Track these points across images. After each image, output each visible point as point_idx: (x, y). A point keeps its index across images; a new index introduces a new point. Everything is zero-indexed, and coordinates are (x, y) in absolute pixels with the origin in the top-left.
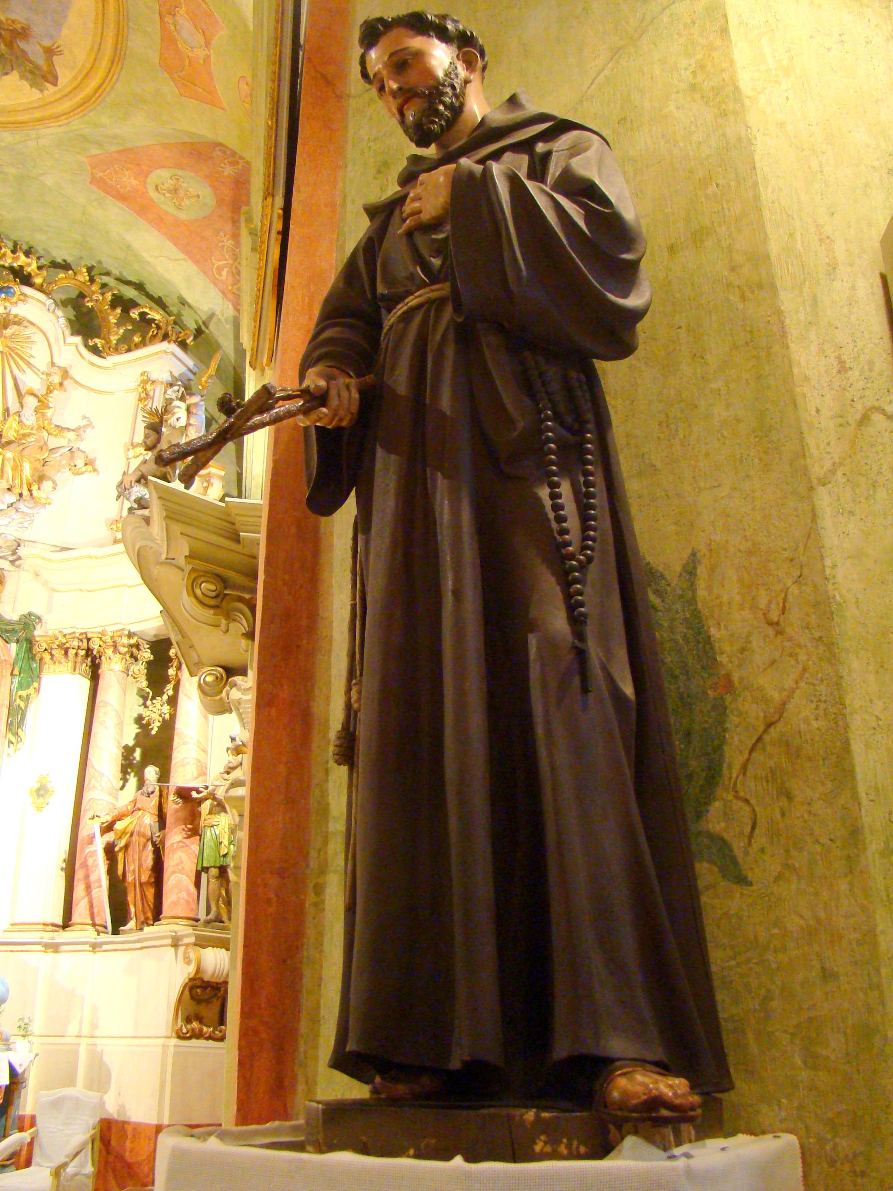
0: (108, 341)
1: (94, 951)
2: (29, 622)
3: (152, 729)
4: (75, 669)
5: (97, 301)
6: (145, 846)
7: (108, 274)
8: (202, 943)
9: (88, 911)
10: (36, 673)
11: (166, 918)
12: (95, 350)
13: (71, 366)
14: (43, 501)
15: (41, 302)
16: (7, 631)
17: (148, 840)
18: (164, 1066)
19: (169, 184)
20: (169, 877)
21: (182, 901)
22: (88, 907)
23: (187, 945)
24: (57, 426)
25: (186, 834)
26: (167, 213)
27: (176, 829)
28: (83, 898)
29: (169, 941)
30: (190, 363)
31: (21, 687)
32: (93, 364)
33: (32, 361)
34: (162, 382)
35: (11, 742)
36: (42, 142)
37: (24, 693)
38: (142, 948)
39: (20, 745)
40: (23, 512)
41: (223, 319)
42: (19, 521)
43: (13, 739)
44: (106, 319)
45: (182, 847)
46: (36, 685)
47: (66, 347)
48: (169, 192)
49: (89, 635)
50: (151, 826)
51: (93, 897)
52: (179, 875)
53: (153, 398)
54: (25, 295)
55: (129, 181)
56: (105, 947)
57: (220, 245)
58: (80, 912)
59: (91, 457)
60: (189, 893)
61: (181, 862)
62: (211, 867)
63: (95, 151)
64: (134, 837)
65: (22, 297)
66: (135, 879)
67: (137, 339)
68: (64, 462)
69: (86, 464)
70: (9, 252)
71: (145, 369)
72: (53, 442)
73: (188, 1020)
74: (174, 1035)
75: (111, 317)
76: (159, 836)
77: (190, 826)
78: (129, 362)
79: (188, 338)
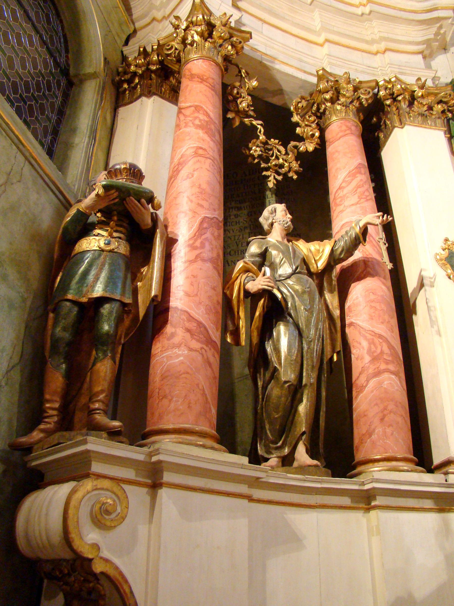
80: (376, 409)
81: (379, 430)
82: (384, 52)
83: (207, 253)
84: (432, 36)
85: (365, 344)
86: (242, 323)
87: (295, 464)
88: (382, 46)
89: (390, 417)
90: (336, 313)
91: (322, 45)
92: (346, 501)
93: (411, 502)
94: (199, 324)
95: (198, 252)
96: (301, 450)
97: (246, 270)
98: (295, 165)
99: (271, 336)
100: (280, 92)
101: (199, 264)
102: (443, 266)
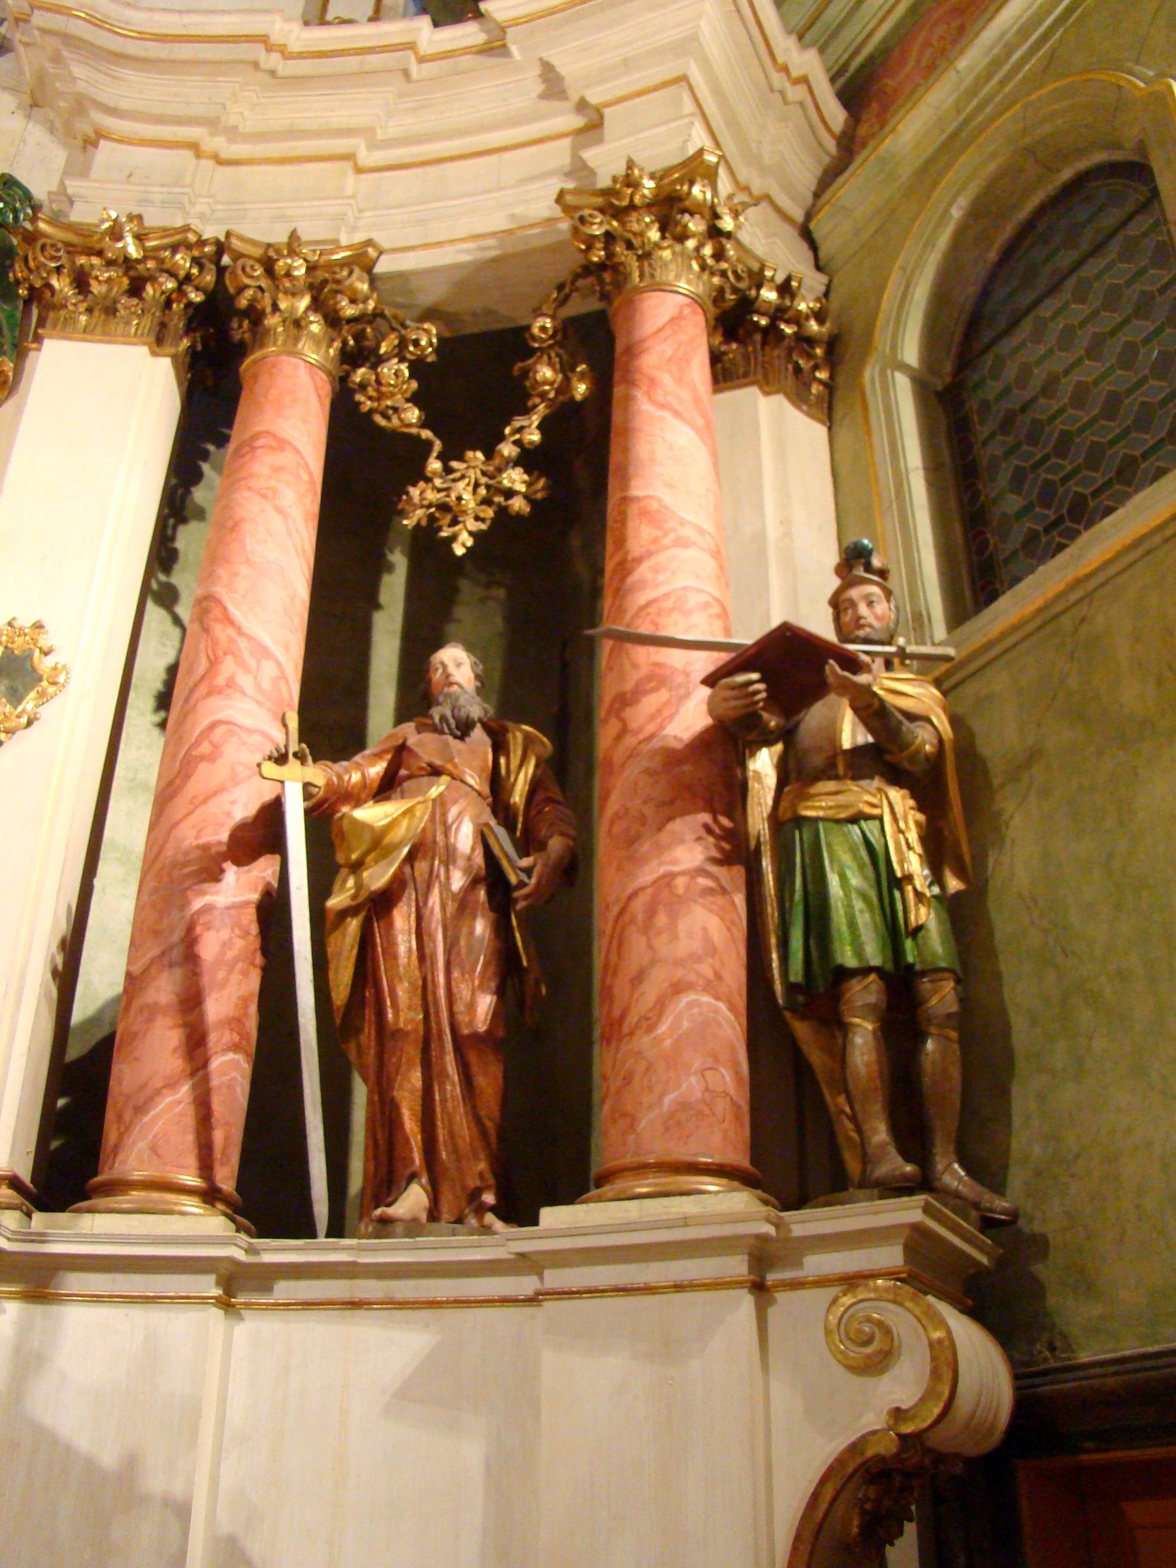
1: (226, 1304)
3: (453, 538)
9: (190, 1137)
11: (642, 1169)
20: (661, 1005)
21: (722, 1106)
22: (190, 1120)
25: (721, 849)
27: (677, 825)
28: (171, 1085)
29: (737, 1266)
45: (708, 891)
51: (215, 1082)
52: (706, 999)
56: (284, 1290)
62: (865, 971)
64: (421, 866)
76: (528, 871)
77: (725, 821)
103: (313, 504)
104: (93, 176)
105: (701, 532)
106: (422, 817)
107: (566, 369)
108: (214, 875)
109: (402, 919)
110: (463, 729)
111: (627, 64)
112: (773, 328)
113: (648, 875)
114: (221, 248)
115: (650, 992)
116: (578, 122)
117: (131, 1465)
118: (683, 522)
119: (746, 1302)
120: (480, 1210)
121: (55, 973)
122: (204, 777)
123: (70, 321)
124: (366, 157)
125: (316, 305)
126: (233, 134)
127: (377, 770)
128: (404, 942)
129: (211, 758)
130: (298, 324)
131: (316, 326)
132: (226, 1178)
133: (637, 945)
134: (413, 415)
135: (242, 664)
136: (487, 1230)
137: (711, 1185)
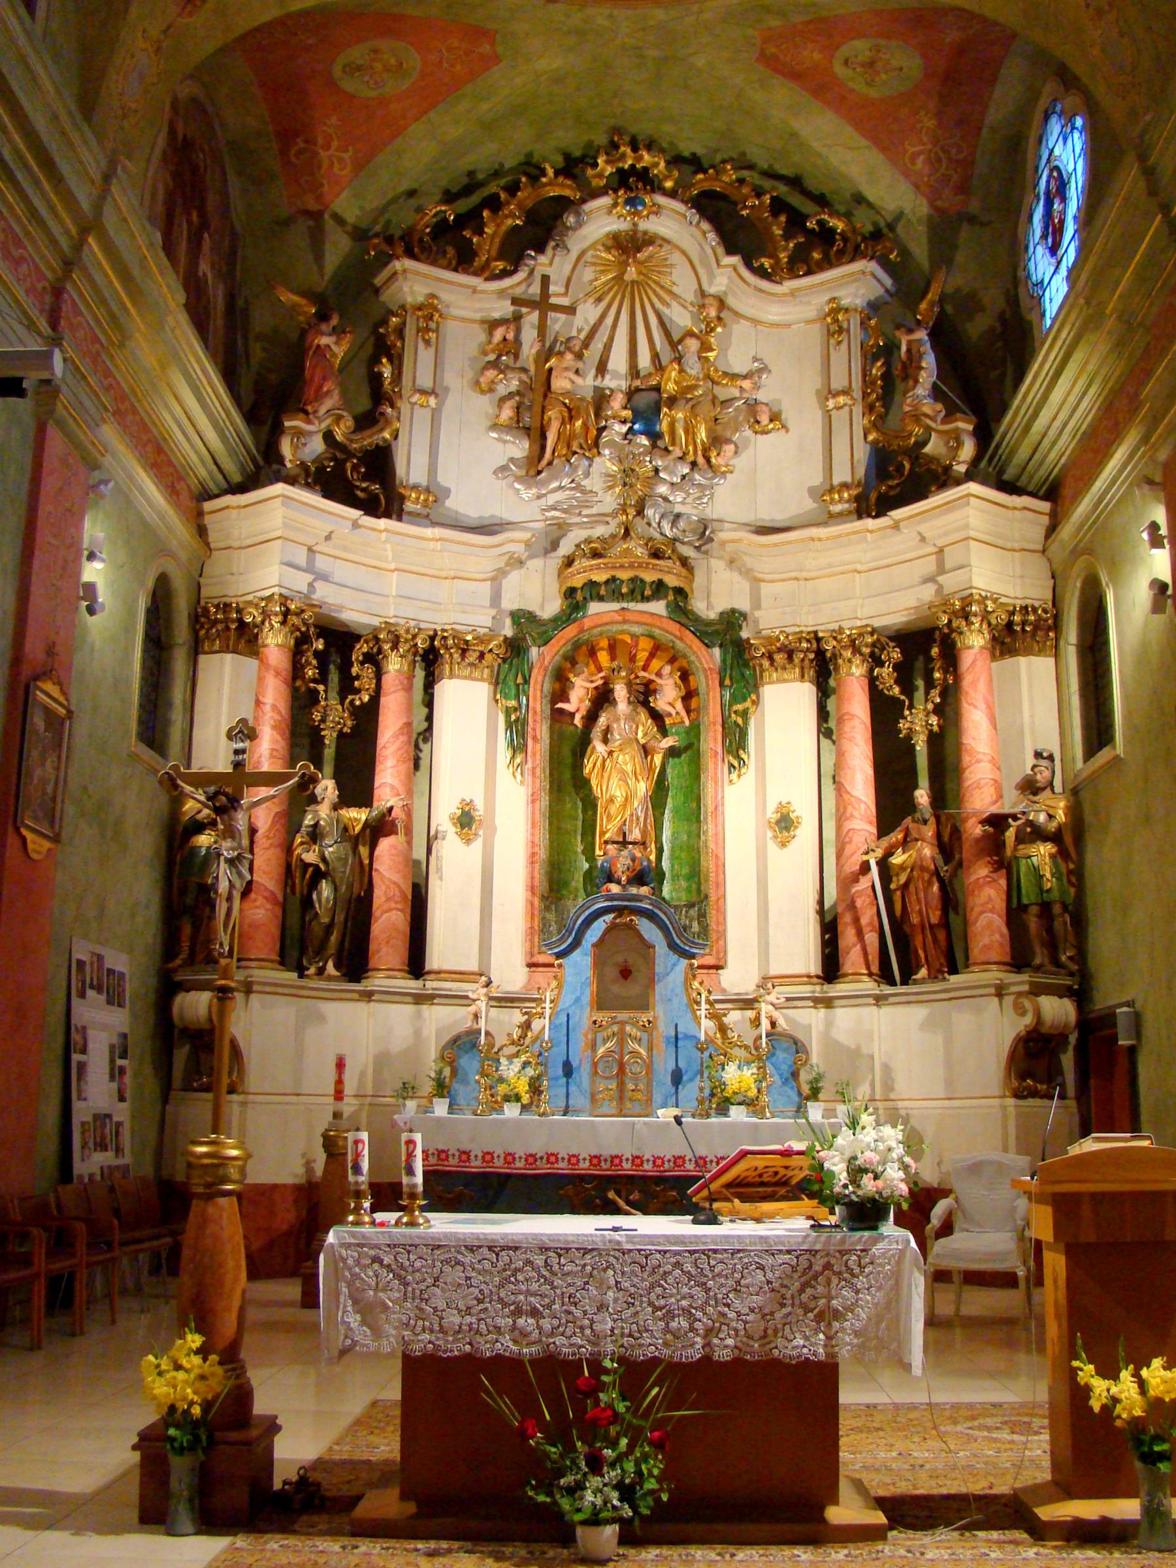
0: (778, 261)
1: (877, 1005)
2: (732, 620)
4: (803, 676)
5: (753, 207)
6: (930, 883)
7: (751, 167)
8: (1036, 990)
10: (751, 681)
11: (975, 964)
12: (761, 273)
13: (725, 293)
14: (724, 469)
15: (678, 213)
16: (706, 633)
17: (932, 876)
18: (1005, 1127)
19: (865, 56)
21: (996, 944)
23: (1019, 994)
24: (725, 374)
26: (852, 91)
27: (979, 863)
28: (855, 945)
29: (993, 991)
30: (888, 282)
31: (734, 699)
32: (761, 291)
33: (675, 289)
34: (856, 310)
35: (731, 766)
36: (707, 16)
37: (739, 707)
38: (950, 999)
39: (743, 770)
40: (700, 484)
41: (914, 220)
42: (696, 495)
43: (736, 764)
44: (768, 229)
46: (754, 697)
47: (721, 270)
48: (863, 65)
49: (820, 635)
50: (933, 859)
53: (848, 331)
54: (659, 207)
55: (812, 55)
56: (892, 1000)
57: (918, 126)
58: (852, 960)
59: (775, 409)
60: (1002, 936)
61: (990, 899)
63: (775, 22)
65: (655, 209)
66: (922, 920)
67: (816, 255)
68: (741, 418)
69: (771, 421)
70: (629, 151)
71: (835, 295)
72: (722, 393)
73: (1022, 1077)
74: (1007, 1093)
75: (775, 228)
77: (995, 858)
78: (814, 286)
79: (891, 253)
80: (384, 936)
81: (384, 950)
82: (454, 578)
83: (276, 841)
84: (503, 565)
85: (384, 888)
86: (297, 881)
87: (326, 973)
88: (452, 573)
89: (393, 942)
90: (366, 862)
91: (393, 571)
92: (356, 996)
93: (397, 998)
94: (272, 893)
95: (270, 842)
96: (330, 964)
97: (302, 843)
98: (349, 723)
99: (316, 888)
100: (347, 626)
101: (272, 850)
102: (454, 824)
103: (868, 735)
104: (764, 604)
105: (984, 754)
106: (914, 855)
107: (945, 672)
108: (856, 881)
109: (912, 888)
110: (925, 822)
111: (946, 534)
112: (1023, 629)
113: (973, 878)
114: (816, 633)
115: (974, 914)
116: (936, 550)
117: (858, 1048)
118: (978, 753)
119: (996, 1000)
120: (943, 973)
121: (817, 912)
122: (848, 850)
123: (770, 676)
124: (859, 567)
125: (853, 653)
126: (809, 571)
127: (900, 836)
128: (914, 898)
129: (850, 842)
130: (850, 661)
131: (857, 660)
132: (875, 969)
133: (971, 899)
134: (896, 690)
135: (854, 807)
136: (944, 979)
137: (994, 967)
